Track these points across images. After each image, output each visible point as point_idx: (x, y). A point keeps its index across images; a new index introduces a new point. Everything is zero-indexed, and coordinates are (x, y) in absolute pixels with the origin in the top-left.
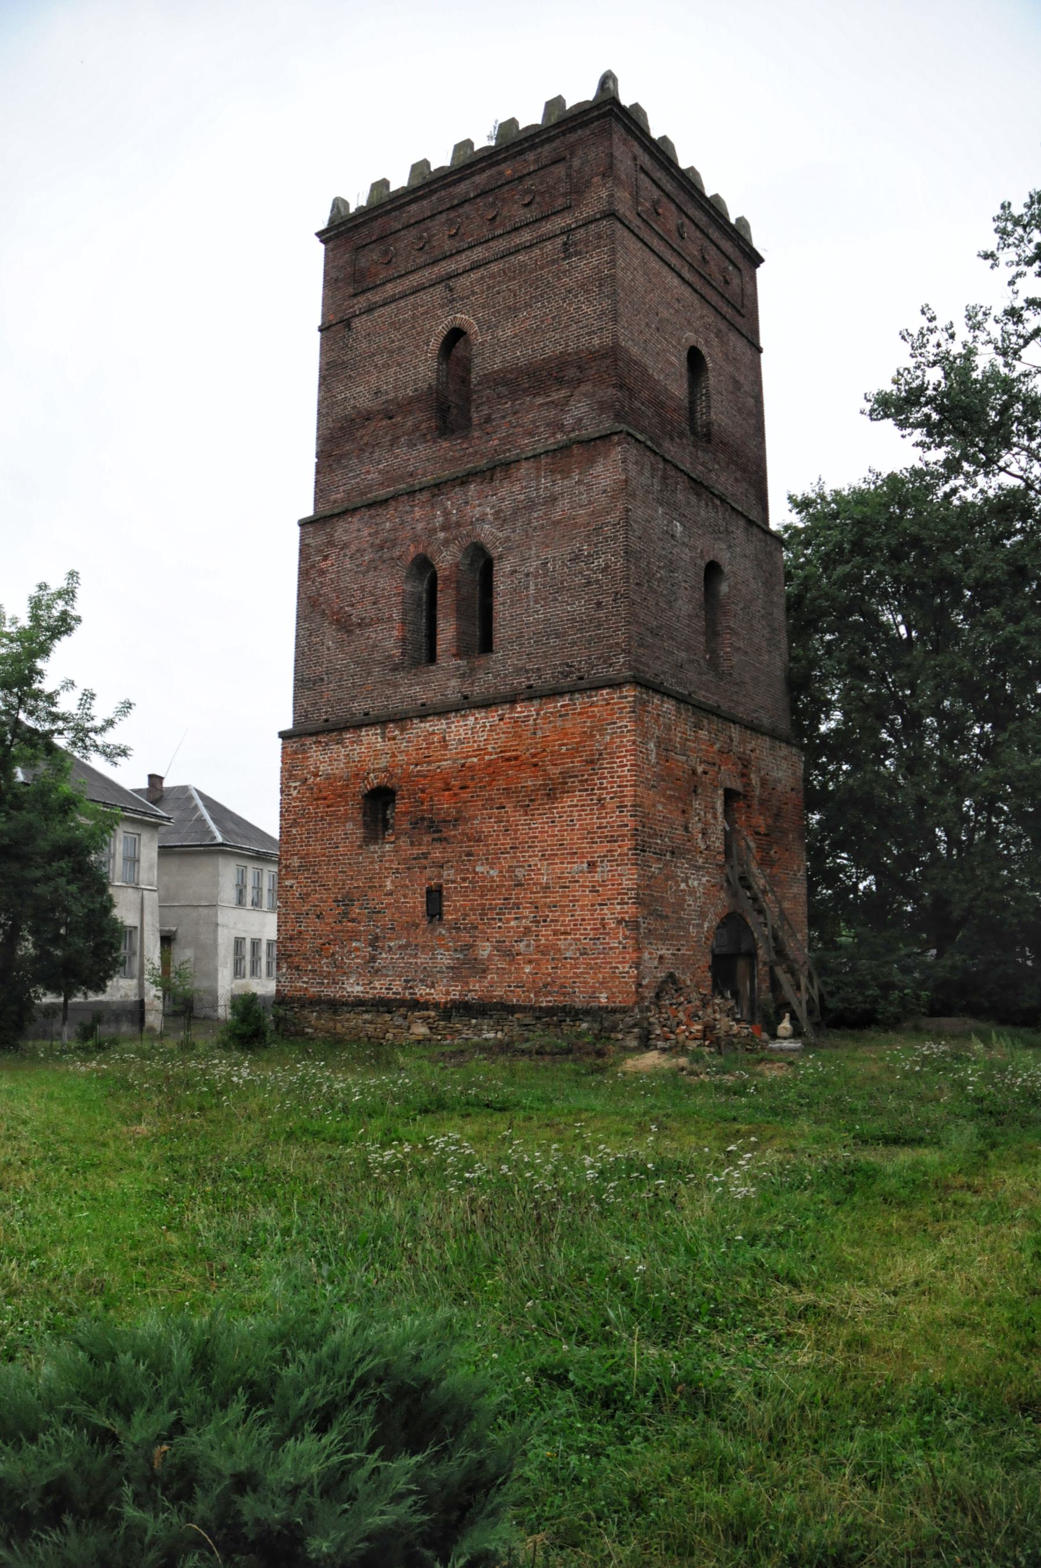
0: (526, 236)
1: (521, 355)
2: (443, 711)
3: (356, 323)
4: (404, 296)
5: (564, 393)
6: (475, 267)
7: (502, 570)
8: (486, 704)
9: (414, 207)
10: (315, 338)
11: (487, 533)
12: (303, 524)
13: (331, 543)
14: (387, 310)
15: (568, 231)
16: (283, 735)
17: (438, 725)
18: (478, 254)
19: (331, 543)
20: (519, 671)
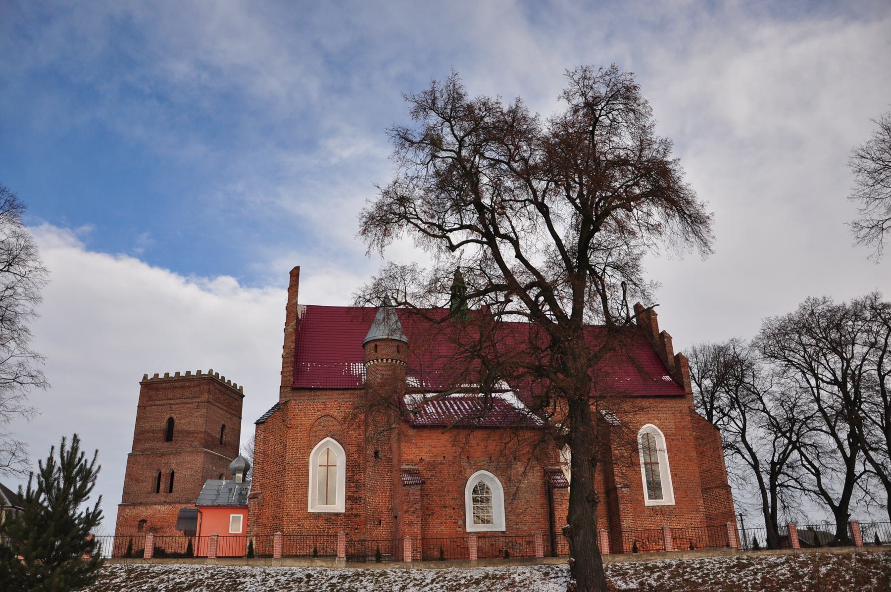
0: (189, 401)
1: (186, 428)
2: (160, 504)
3: (147, 408)
4: (160, 405)
5: (193, 439)
6: (177, 404)
7: (176, 475)
8: (170, 504)
9: (164, 384)
10: (136, 408)
11: (173, 466)
12: (129, 455)
13: (136, 461)
14: (155, 407)
15: (198, 402)
16: (119, 505)
17: (158, 507)
18: (178, 401)
19: (136, 461)
20: (177, 497)
